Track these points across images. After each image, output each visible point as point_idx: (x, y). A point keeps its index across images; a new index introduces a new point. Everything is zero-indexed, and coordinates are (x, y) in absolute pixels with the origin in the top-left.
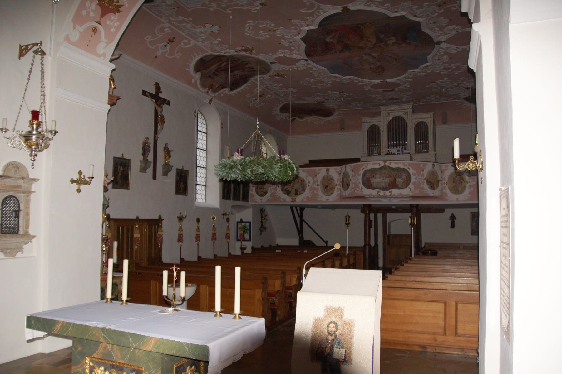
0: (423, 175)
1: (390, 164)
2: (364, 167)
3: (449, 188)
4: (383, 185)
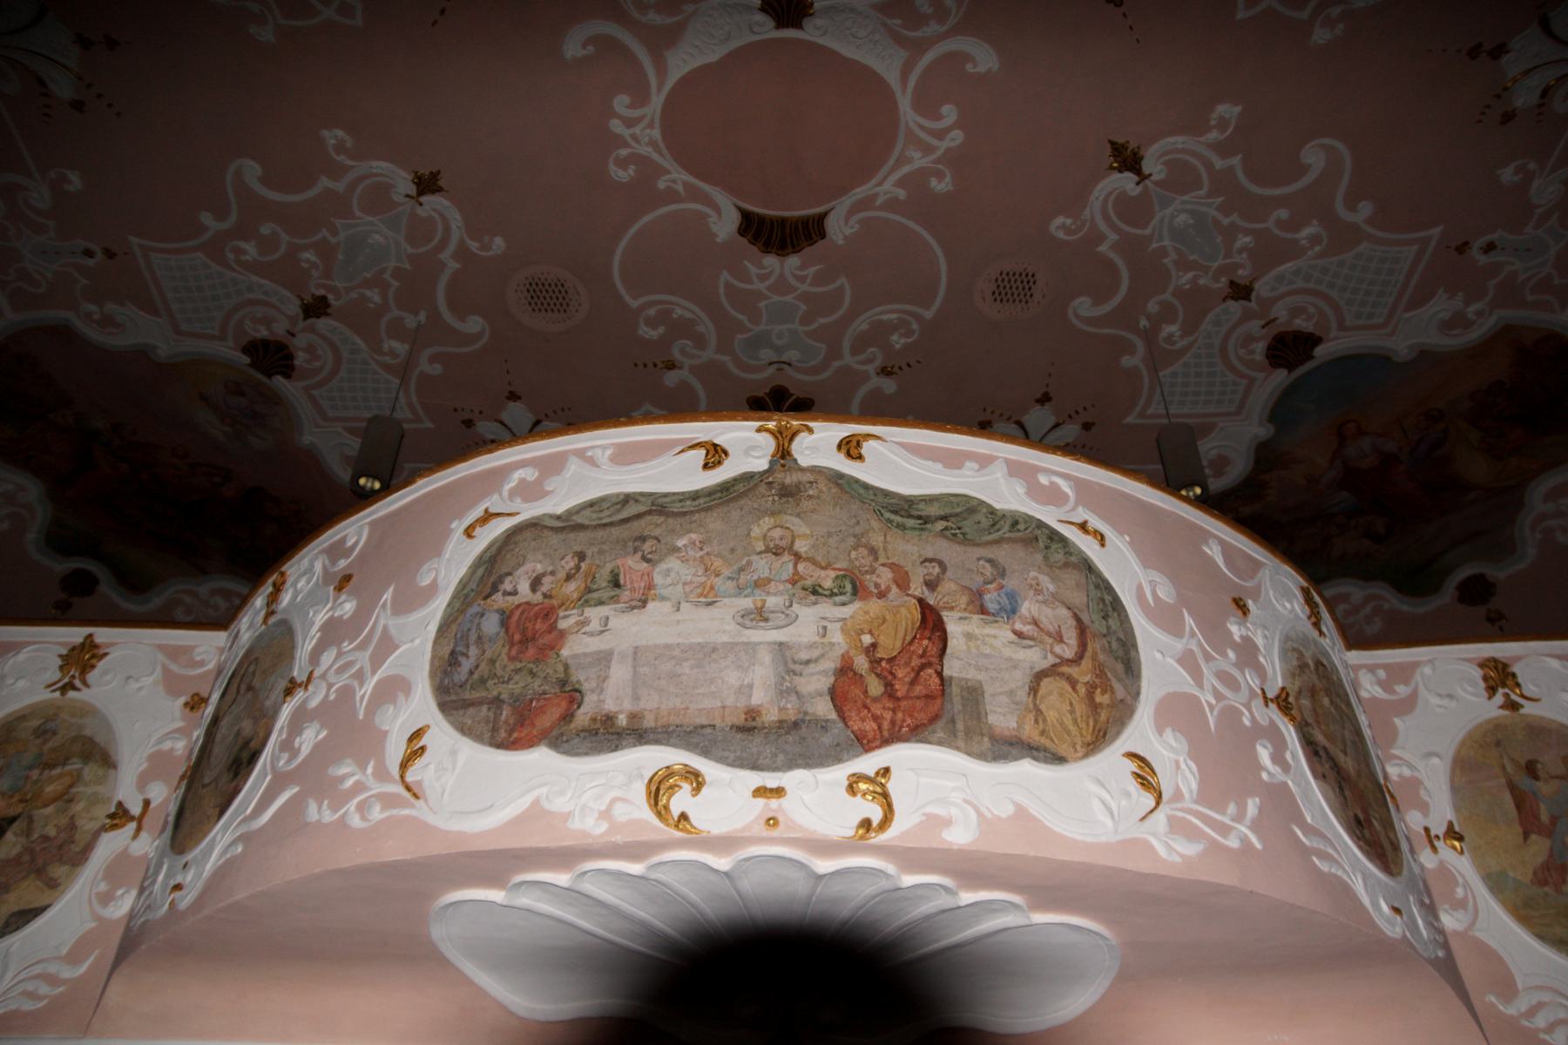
0: (1247, 653)
1: (850, 448)
2: (493, 503)
3: (1496, 883)
4: (757, 686)
